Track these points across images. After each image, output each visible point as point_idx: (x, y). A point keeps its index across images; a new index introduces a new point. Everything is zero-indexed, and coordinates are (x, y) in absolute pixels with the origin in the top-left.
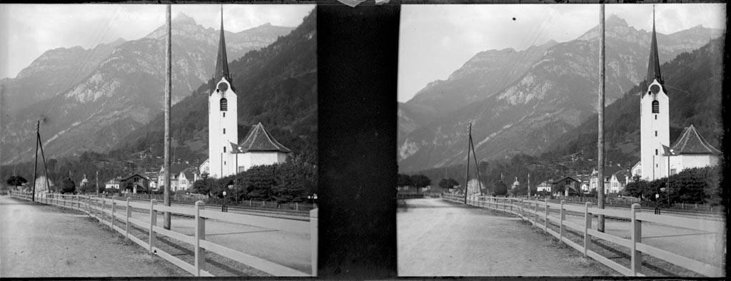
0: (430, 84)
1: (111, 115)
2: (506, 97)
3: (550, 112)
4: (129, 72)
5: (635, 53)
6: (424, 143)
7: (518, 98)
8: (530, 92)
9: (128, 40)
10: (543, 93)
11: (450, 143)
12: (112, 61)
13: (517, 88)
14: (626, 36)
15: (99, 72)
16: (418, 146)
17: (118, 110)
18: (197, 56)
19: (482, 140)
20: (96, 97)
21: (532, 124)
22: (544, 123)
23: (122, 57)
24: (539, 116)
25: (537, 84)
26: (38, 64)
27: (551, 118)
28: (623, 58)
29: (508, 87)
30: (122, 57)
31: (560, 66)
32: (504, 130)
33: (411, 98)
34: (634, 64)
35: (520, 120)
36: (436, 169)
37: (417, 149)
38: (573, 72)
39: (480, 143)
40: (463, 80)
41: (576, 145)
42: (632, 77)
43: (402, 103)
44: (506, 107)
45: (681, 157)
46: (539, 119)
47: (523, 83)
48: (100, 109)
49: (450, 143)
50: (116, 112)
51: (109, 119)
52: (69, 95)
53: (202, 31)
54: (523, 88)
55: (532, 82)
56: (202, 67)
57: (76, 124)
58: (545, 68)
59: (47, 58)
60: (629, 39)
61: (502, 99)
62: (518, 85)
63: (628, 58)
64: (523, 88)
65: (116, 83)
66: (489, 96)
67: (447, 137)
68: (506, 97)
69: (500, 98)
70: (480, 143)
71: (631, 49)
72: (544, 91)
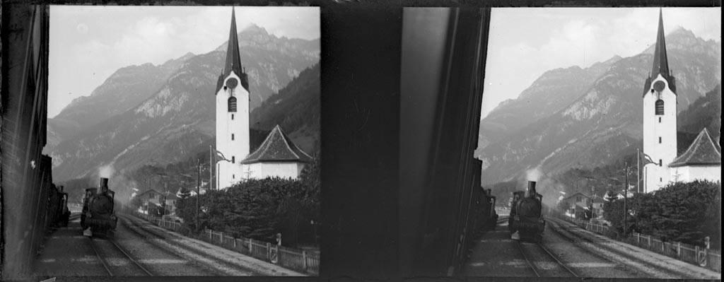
0: (75, 100)
1: (179, 129)
2: (571, 113)
3: (613, 126)
4: (198, 85)
5: (275, 61)
6: (68, 155)
7: (582, 114)
8: (168, 104)
9: (197, 54)
10: (607, 108)
11: (518, 158)
12: (180, 75)
13: (581, 104)
14: (693, 46)
15: (167, 87)
16: (489, 162)
17: (186, 124)
18: (268, 66)
19: (547, 155)
20: (164, 112)
21: (595, 138)
22: (606, 138)
23: (190, 71)
24: (176, 127)
25: (601, 99)
26: (111, 81)
27: (188, 129)
28: (690, 69)
29: (574, 103)
30: (190, 71)
31: (197, 78)
32: (569, 145)
33: (57, 114)
34: (701, 75)
35: (157, 133)
36: (80, 180)
37: (489, 164)
38: (637, 86)
39: (119, 155)
40: (532, 97)
41: (631, 159)
42: (700, 88)
43: (50, 119)
44: (571, 123)
45: (260, 165)
46: (176, 130)
47: (587, 98)
48: (169, 123)
49: (518, 158)
50: (184, 125)
51: (178, 132)
52: (139, 110)
53: (275, 40)
54: (161, 101)
55: (169, 94)
56: (274, 77)
57: (146, 138)
58: (609, 83)
59: (118, 76)
60: (269, 47)
61: (567, 115)
62: (156, 98)
63: (695, 69)
64: (161, 101)
65: (184, 97)
66: (128, 110)
67: (88, 150)
68: (571, 113)
69: (139, 110)
70: (119, 155)
71: (698, 60)
72: (181, 102)
